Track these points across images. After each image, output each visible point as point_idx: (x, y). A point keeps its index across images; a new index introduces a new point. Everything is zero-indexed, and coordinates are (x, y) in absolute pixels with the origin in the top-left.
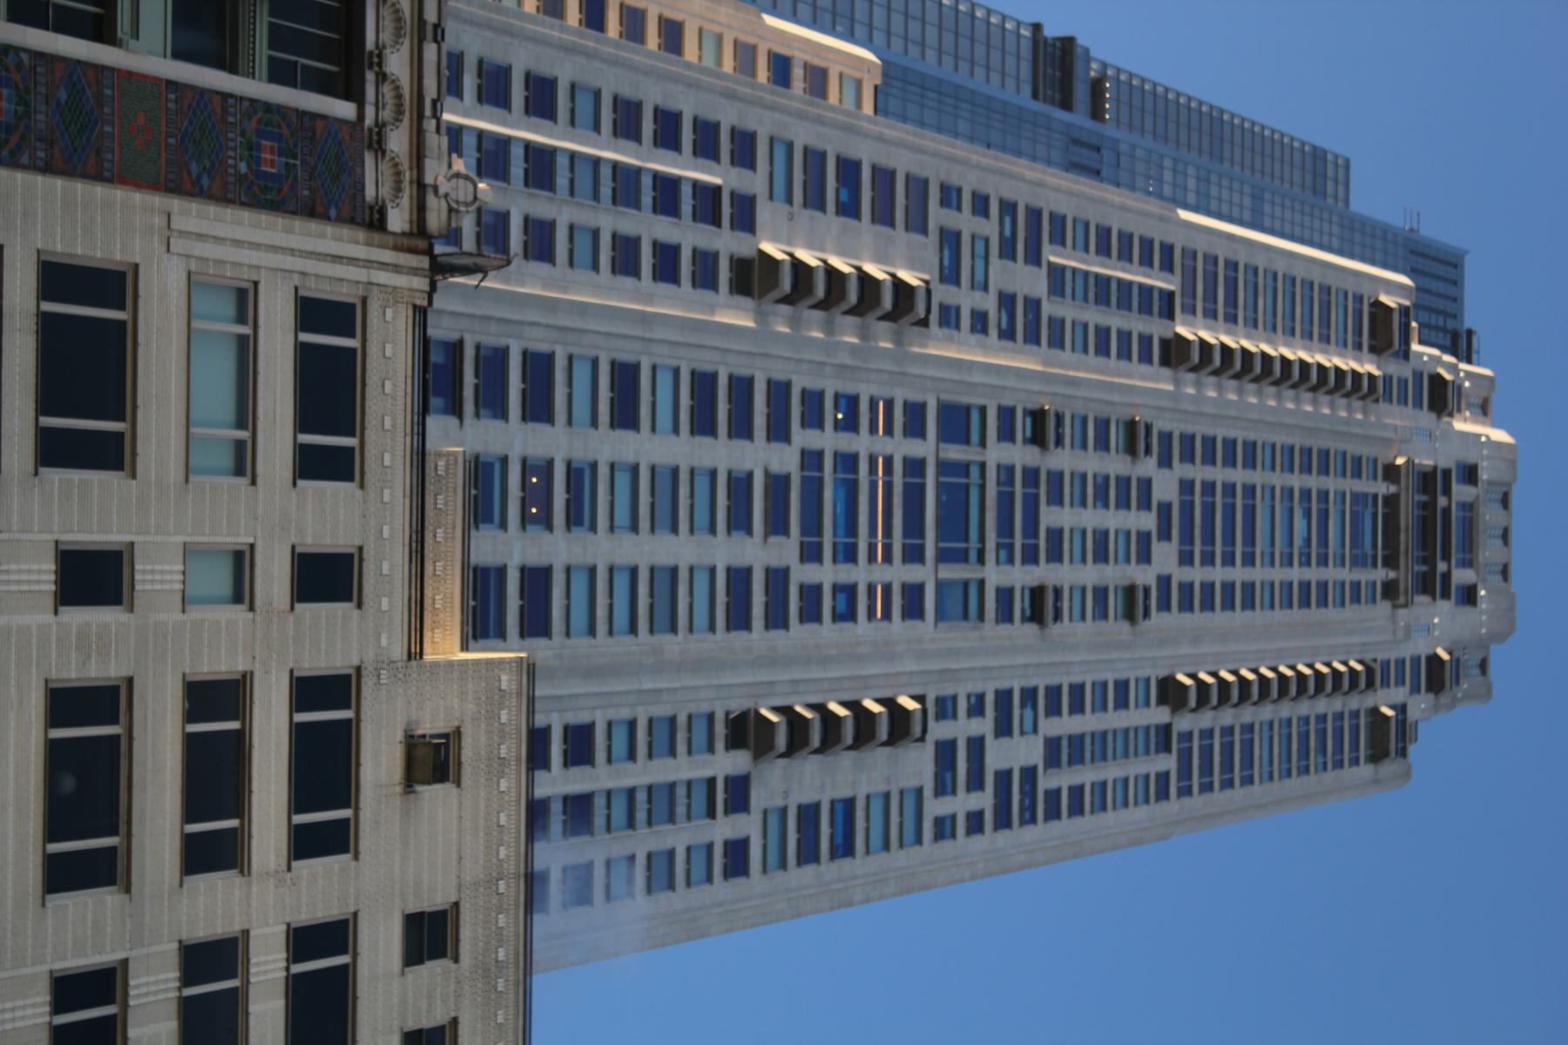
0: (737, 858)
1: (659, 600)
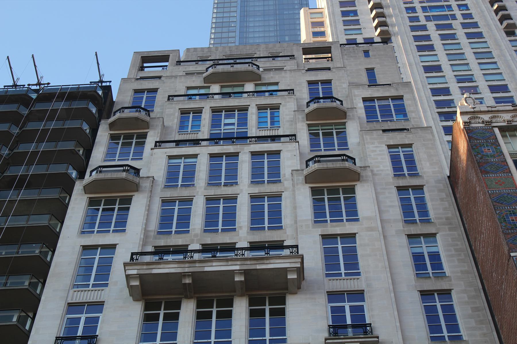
1: (484, 56)
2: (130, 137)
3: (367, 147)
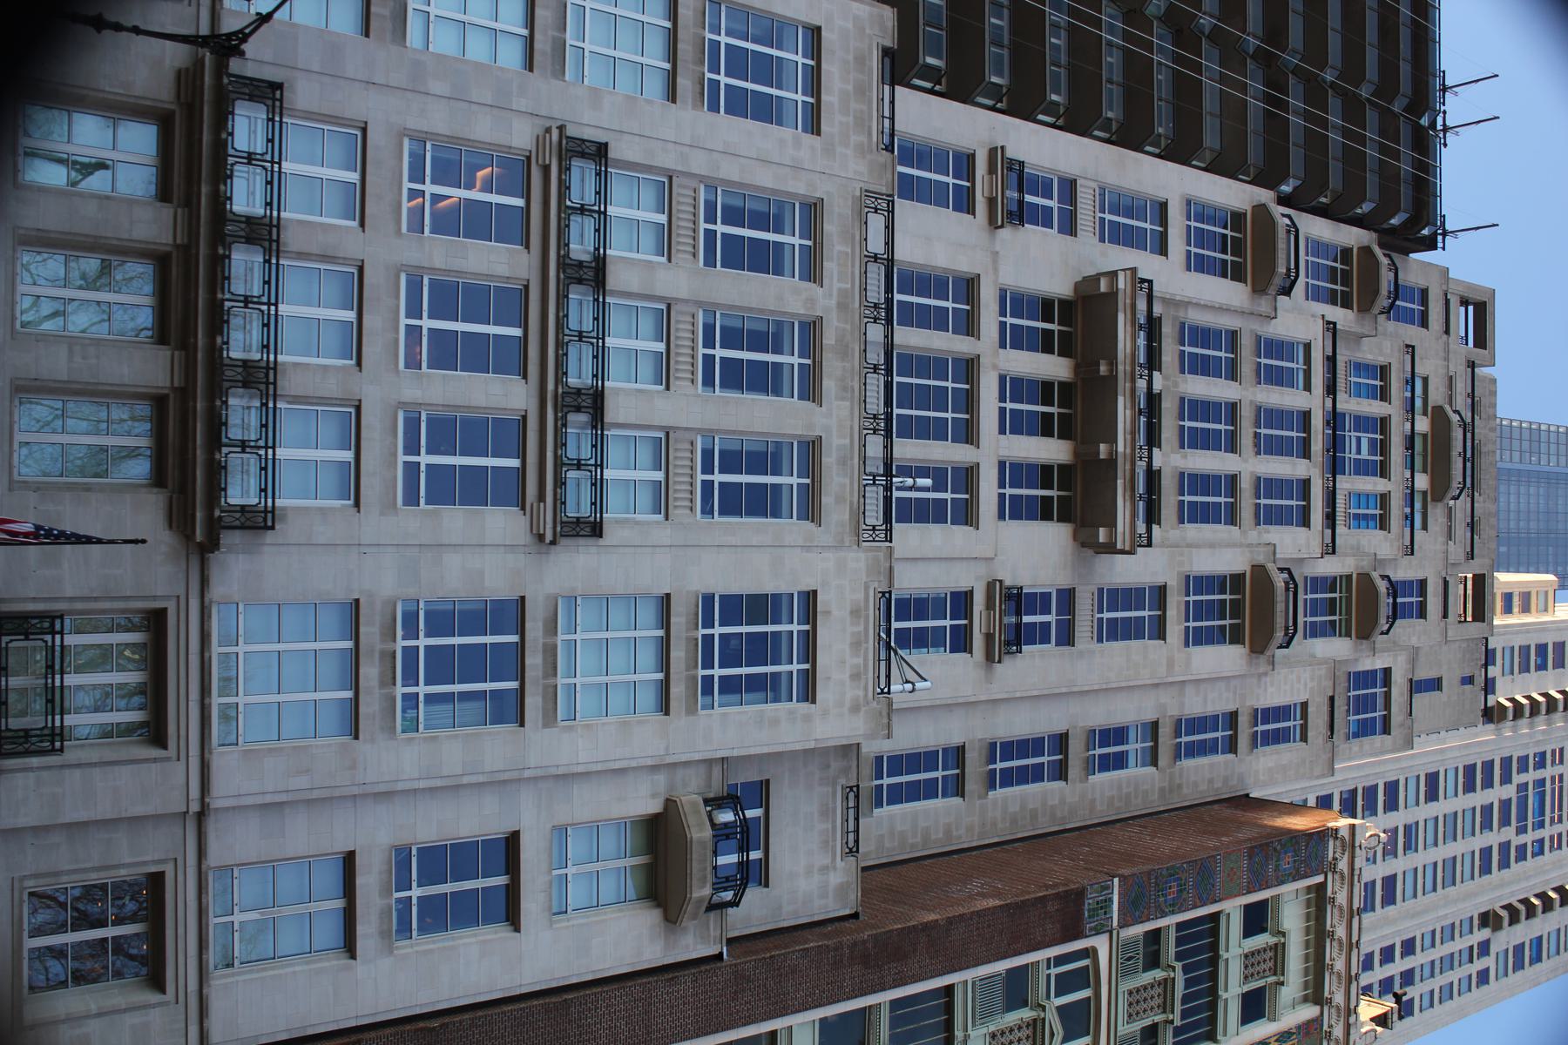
0: (1483, 977)
1: (1449, 873)
2: (1346, 278)
3: (1306, 670)
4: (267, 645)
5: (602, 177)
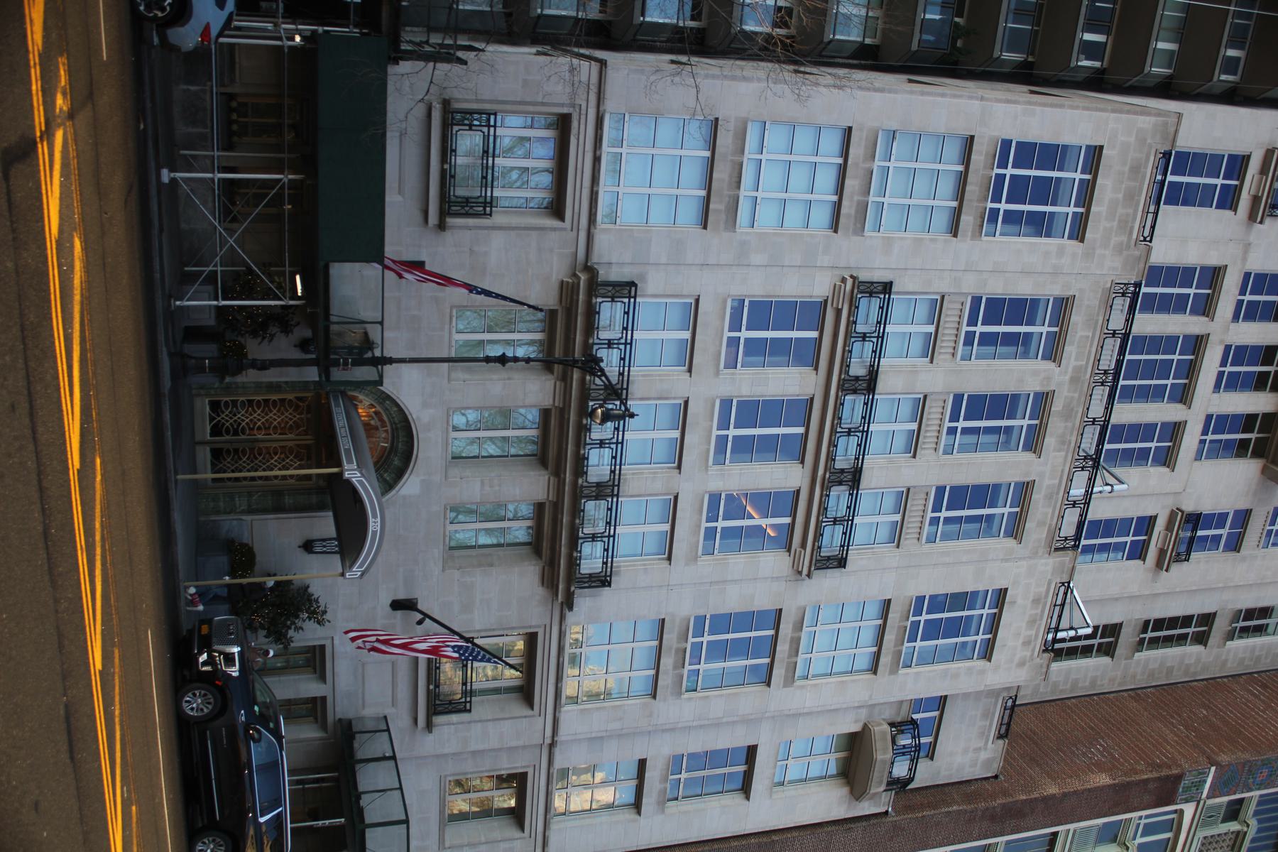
4: (603, 648)
5: (884, 309)
